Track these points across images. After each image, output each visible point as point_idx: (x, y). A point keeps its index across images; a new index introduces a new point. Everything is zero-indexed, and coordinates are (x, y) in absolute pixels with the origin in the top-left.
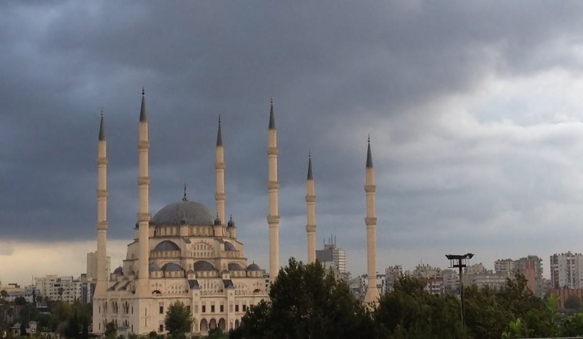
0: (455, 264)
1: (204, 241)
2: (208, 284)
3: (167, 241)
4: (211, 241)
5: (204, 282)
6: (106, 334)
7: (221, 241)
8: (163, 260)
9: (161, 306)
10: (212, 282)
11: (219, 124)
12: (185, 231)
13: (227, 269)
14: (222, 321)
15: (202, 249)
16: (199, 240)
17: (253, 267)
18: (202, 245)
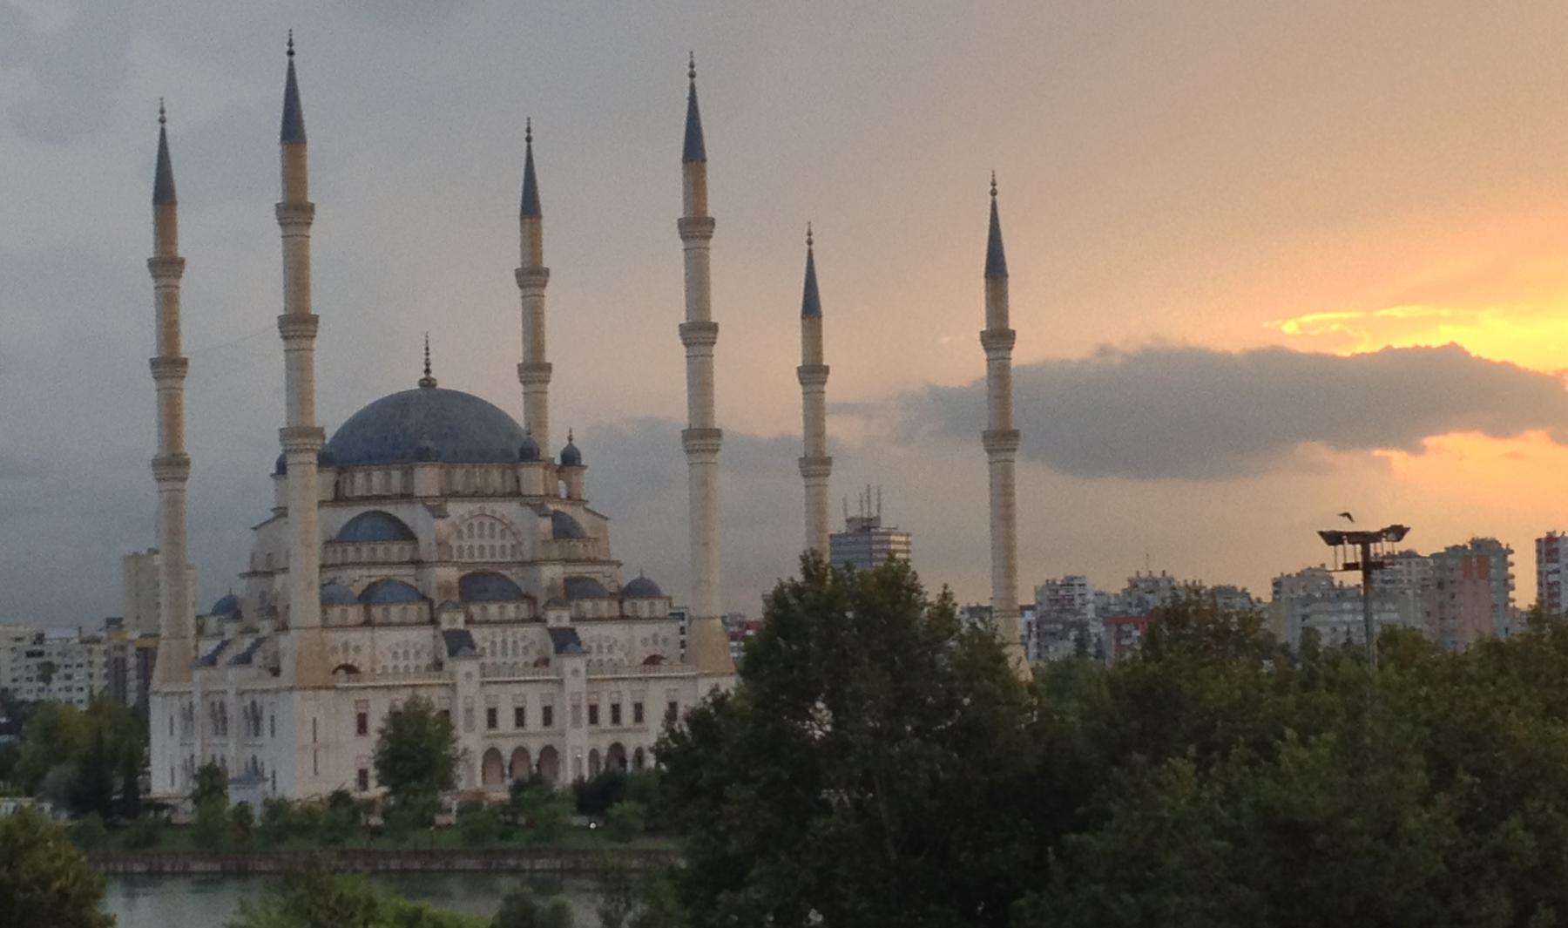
0: (1350, 560)
2: (504, 642)
3: (375, 513)
4: (509, 510)
6: (196, 798)
7: (541, 511)
8: (365, 572)
9: (362, 711)
11: (529, 148)
12: (427, 479)
13: (561, 593)
14: (549, 753)
17: (642, 589)
18: (481, 524)
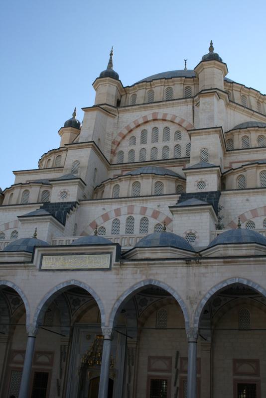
1: (160, 117)
2: (130, 220)
5: (113, 215)
10: (144, 209)
16: (148, 114)
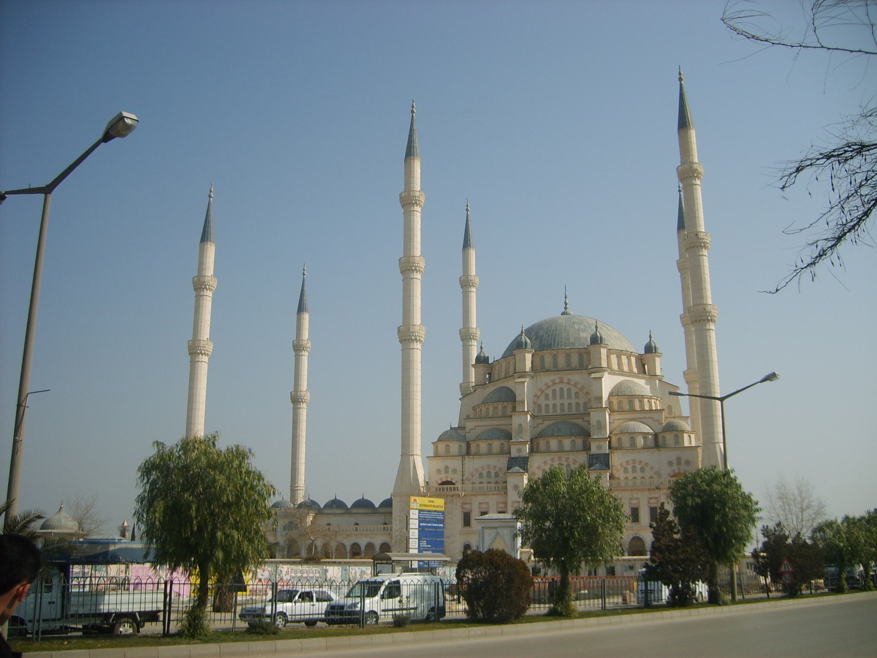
10: (567, 459)
15: (562, 397)
16: (556, 377)
18: (561, 389)
